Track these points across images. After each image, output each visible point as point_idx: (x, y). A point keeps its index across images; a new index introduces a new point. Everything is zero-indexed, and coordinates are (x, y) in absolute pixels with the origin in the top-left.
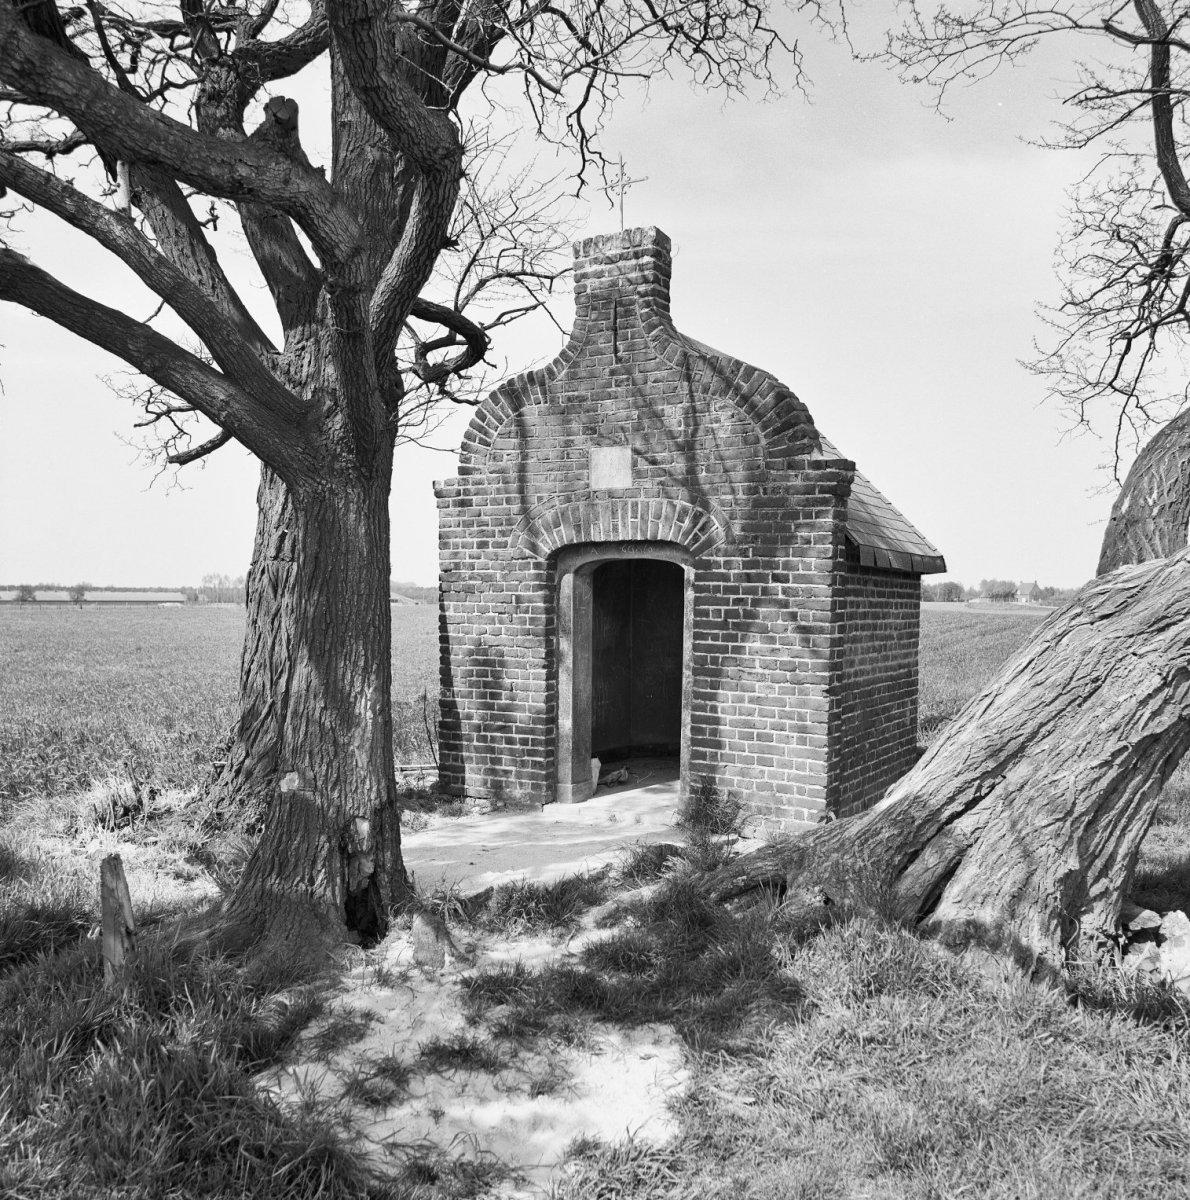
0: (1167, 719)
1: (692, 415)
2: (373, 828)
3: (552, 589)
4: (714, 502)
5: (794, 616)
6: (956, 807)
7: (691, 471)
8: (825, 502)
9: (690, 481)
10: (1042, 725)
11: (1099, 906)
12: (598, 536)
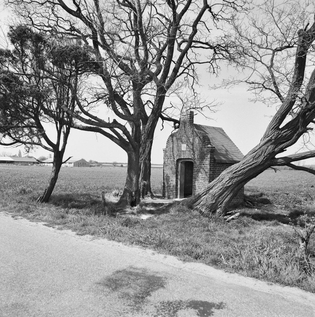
0: (230, 184)
1: (194, 140)
2: (135, 193)
3: (177, 165)
4: (196, 153)
5: (205, 170)
6: (203, 195)
7: (193, 148)
8: (209, 153)
9: (193, 150)
10: (215, 185)
11: (220, 209)
12: (182, 158)
